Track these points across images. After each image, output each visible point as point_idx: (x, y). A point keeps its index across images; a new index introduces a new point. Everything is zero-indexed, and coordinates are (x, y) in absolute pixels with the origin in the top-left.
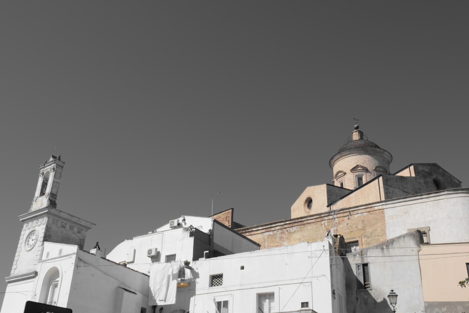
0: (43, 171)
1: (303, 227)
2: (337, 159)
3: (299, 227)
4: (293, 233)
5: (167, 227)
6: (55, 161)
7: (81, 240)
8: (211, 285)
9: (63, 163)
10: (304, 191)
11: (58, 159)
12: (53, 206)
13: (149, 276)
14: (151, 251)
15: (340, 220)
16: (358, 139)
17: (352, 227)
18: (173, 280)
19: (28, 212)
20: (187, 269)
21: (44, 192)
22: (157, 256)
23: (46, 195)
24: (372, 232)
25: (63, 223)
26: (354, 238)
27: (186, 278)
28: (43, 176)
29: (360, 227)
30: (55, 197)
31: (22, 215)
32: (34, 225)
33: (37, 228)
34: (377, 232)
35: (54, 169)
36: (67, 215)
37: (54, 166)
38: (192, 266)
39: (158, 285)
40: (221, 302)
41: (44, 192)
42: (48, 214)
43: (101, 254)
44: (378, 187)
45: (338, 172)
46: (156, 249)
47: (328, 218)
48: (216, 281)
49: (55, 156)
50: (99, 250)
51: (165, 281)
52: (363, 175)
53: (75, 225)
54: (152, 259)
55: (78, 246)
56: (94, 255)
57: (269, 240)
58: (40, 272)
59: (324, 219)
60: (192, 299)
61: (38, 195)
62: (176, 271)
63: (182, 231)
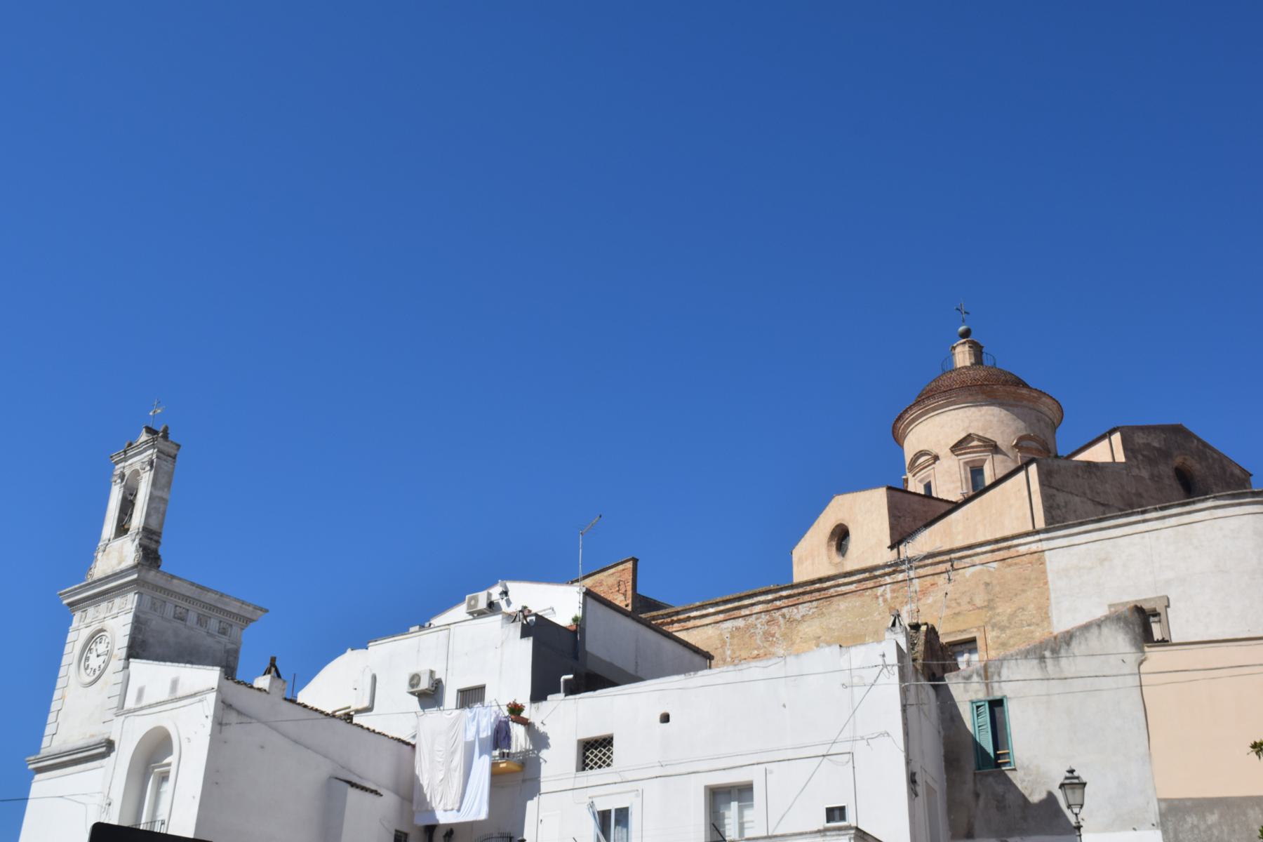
0: (122, 470)
1: (825, 603)
2: (913, 421)
3: (815, 604)
4: (799, 622)
5: (460, 612)
6: (154, 441)
7: (228, 652)
8: (581, 767)
9: (176, 448)
10: (827, 508)
11: (162, 437)
12: (151, 564)
13: (414, 746)
14: (418, 678)
16: (968, 364)
17: (958, 601)
18: (480, 755)
19: (85, 581)
20: (515, 724)
21: (126, 527)
22: (433, 691)
23: (131, 534)
24: (1014, 615)
25: (180, 607)
26: (965, 630)
27: (513, 750)
28: (123, 483)
29: (979, 601)
30: (155, 538)
31: (67, 590)
32: (102, 616)
33: (109, 624)
34: (1026, 613)
35: (151, 463)
36: (191, 587)
37: (152, 454)
38: (530, 716)
39: (441, 770)
40: (609, 811)
41: (126, 527)
42: (137, 584)
43: (284, 690)
44: (1026, 493)
45: (916, 455)
46: (432, 673)
47: (893, 579)
48: (596, 756)
49: (154, 428)
50: (277, 678)
51: (458, 759)
52: (986, 460)
53: (211, 612)
54: (420, 701)
55: (220, 670)
56: (264, 694)
57: (736, 641)
58: (120, 740)
59: (882, 583)
60: (531, 805)
61: (111, 534)
62: (487, 732)
63: (500, 623)
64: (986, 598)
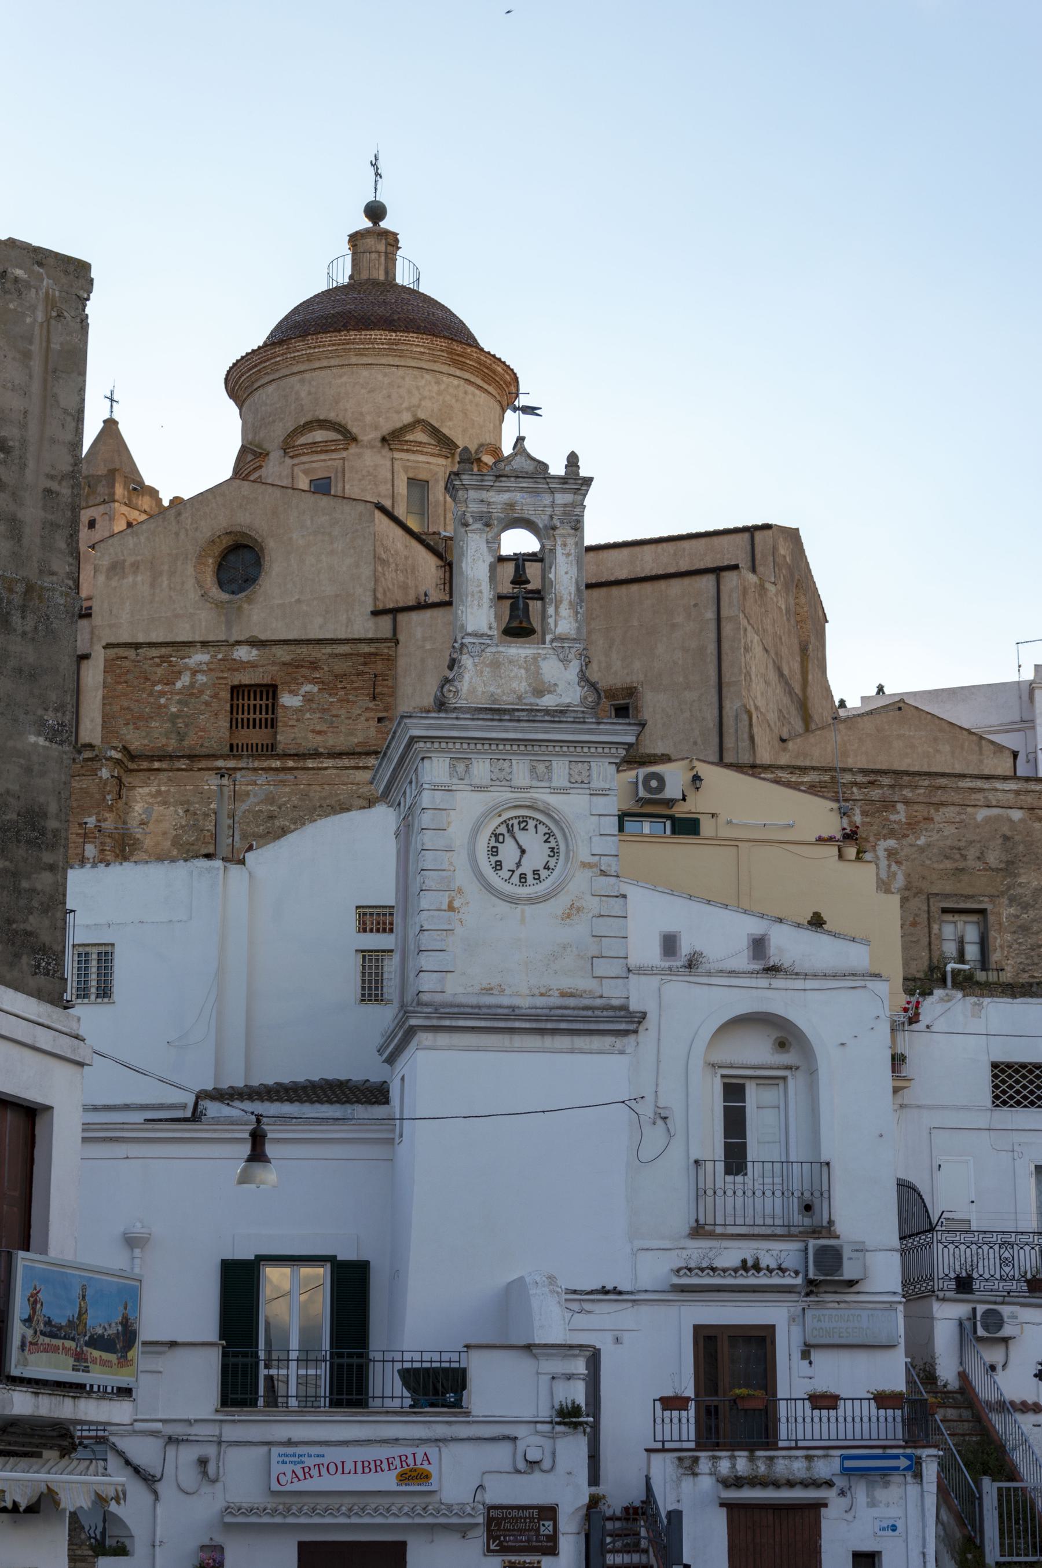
15: (916, 816)
17: (963, 852)
26: (972, 897)
29: (993, 858)
64: (1004, 859)
